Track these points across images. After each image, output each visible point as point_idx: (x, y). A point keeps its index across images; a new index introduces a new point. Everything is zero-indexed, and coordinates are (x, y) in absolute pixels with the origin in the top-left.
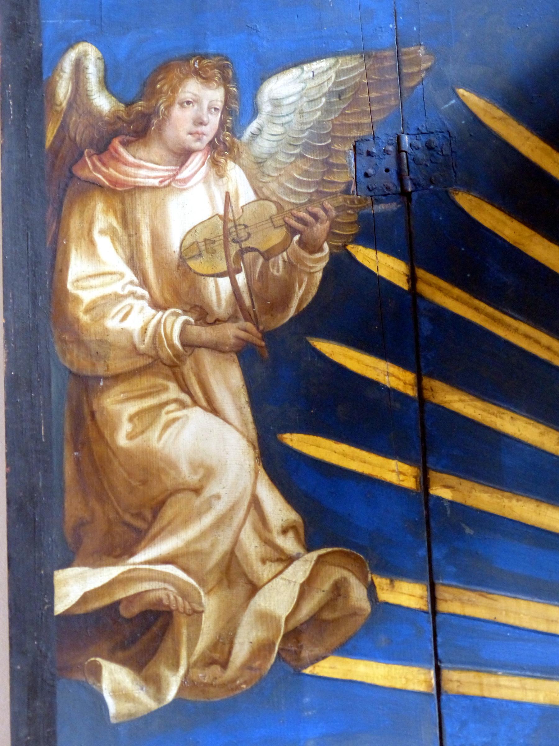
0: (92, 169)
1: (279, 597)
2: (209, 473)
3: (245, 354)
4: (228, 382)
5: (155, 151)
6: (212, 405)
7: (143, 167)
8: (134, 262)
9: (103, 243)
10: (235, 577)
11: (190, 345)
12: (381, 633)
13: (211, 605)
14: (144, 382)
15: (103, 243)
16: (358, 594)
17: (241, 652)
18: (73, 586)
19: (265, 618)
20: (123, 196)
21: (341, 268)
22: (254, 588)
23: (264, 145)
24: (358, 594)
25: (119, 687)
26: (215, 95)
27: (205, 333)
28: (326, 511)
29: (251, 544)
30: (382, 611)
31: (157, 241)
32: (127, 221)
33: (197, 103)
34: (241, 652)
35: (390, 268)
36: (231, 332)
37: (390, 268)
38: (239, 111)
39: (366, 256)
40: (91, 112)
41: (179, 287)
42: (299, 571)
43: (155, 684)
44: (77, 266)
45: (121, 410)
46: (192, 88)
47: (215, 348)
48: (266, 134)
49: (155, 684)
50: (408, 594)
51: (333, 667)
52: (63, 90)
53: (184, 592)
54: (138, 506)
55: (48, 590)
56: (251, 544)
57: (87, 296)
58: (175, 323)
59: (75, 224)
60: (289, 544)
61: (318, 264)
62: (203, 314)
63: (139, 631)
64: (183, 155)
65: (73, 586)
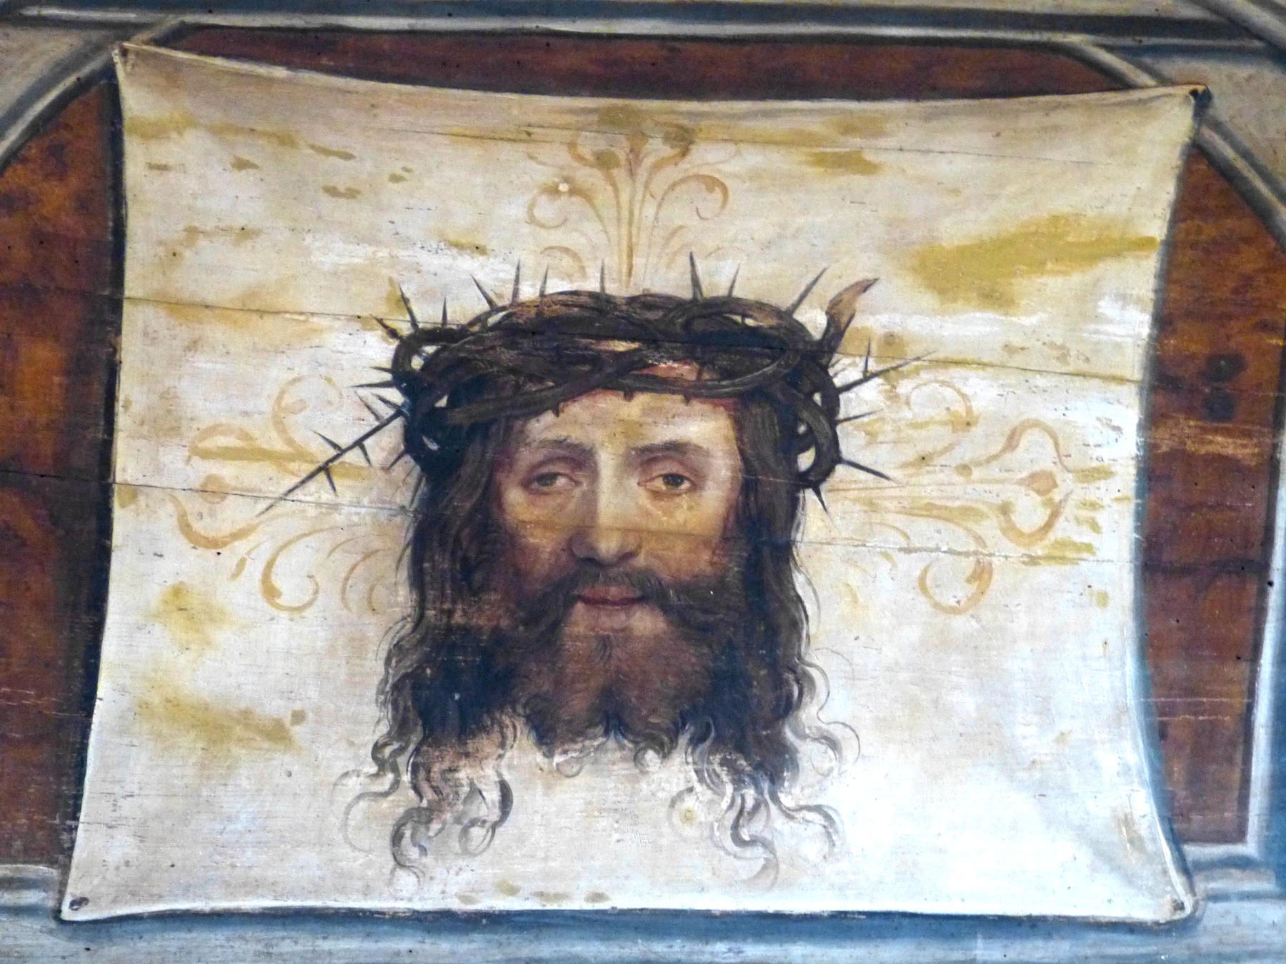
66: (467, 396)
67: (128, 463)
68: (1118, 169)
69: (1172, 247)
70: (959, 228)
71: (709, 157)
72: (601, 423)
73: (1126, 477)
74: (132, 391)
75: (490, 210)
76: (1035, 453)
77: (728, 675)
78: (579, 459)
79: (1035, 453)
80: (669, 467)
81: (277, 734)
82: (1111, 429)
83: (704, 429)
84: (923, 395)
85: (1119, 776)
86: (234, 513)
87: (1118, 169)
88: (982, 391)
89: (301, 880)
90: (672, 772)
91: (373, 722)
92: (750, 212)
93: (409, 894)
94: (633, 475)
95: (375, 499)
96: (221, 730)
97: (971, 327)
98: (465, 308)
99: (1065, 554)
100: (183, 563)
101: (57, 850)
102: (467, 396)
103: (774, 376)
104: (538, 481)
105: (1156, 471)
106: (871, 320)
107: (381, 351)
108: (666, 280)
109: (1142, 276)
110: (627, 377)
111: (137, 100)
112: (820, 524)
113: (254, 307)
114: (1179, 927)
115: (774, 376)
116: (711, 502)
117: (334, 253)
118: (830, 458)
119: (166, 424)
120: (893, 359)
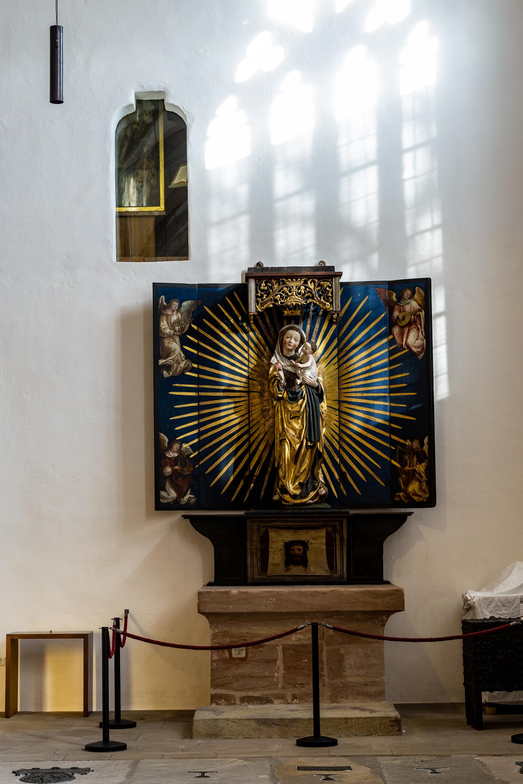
0: (163, 312)
1: (182, 365)
2: (175, 350)
3: (180, 336)
4: (177, 339)
5: (170, 310)
6: (121, 200)
7: (169, 312)
8: (168, 324)
9: (165, 321)
10: (178, 363)
11: (174, 334)
12: (193, 370)
13: (175, 365)
14: (168, 339)
15: (165, 321)
16: (190, 365)
17: (178, 371)
18: (161, 362)
19: (181, 367)
20: (167, 315)
21: (190, 327)
22: (180, 364)
23: (182, 311)
24: (190, 365)
25: (165, 373)
26: (177, 304)
27: (176, 333)
28: (188, 356)
29: (179, 359)
30: (193, 367)
31: (170, 321)
32: (167, 318)
33: (175, 304)
34: (178, 371)
35: (195, 327)
36: (178, 333)
37: (195, 327)
38: (180, 306)
39: (193, 326)
40: (163, 304)
41: (172, 326)
42: (184, 362)
43: (169, 374)
44: (162, 324)
45: (166, 341)
46: (175, 303)
47: (176, 335)
48: (183, 309)
49: (169, 374)
50: (195, 366)
51: (188, 373)
52: (160, 301)
53: (172, 363)
54: (168, 353)
55: (158, 362)
56: (179, 359)
57: (163, 328)
58: (172, 332)
59: (161, 318)
60: (183, 359)
61: (188, 326)
62: (175, 331)
63: (168, 367)
64: (173, 311)
65: (161, 362)
66: (288, 546)
67: (270, 550)
68: (323, 533)
69: (326, 537)
70: (314, 536)
71: (300, 533)
72: (296, 547)
73: (325, 550)
74: (270, 546)
75: (288, 536)
76: (320, 548)
77: (303, 561)
78: (294, 549)
79: (320, 548)
80: (299, 550)
81: (279, 565)
82: (324, 547)
83: (301, 547)
84: (313, 545)
85: (326, 567)
86: (276, 553)
87: (323, 533)
88: (316, 545)
89: (280, 573)
90: (301, 567)
91: (284, 564)
92: (303, 536)
93: (286, 574)
94: (297, 550)
95: (283, 552)
96: (275, 565)
97: (315, 542)
98: (288, 541)
99: (322, 554)
100: (273, 555)
101: (266, 571)
102: (288, 546)
103: (305, 545)
104: (292, 551)
105: (326, 549)
106: (310, 541)
107: (283, 544)
108: (298, 539)
109: (325, 538)
110: (297, 545)
111: (269, 531)
112: (308, 552)
113: (276, 541)
114: (331, 576)
115: (305, 545)
116: (302, 552)
117: (280, 538)
118: (308, 549)
119: (272, 548)
120: (311, 543)
